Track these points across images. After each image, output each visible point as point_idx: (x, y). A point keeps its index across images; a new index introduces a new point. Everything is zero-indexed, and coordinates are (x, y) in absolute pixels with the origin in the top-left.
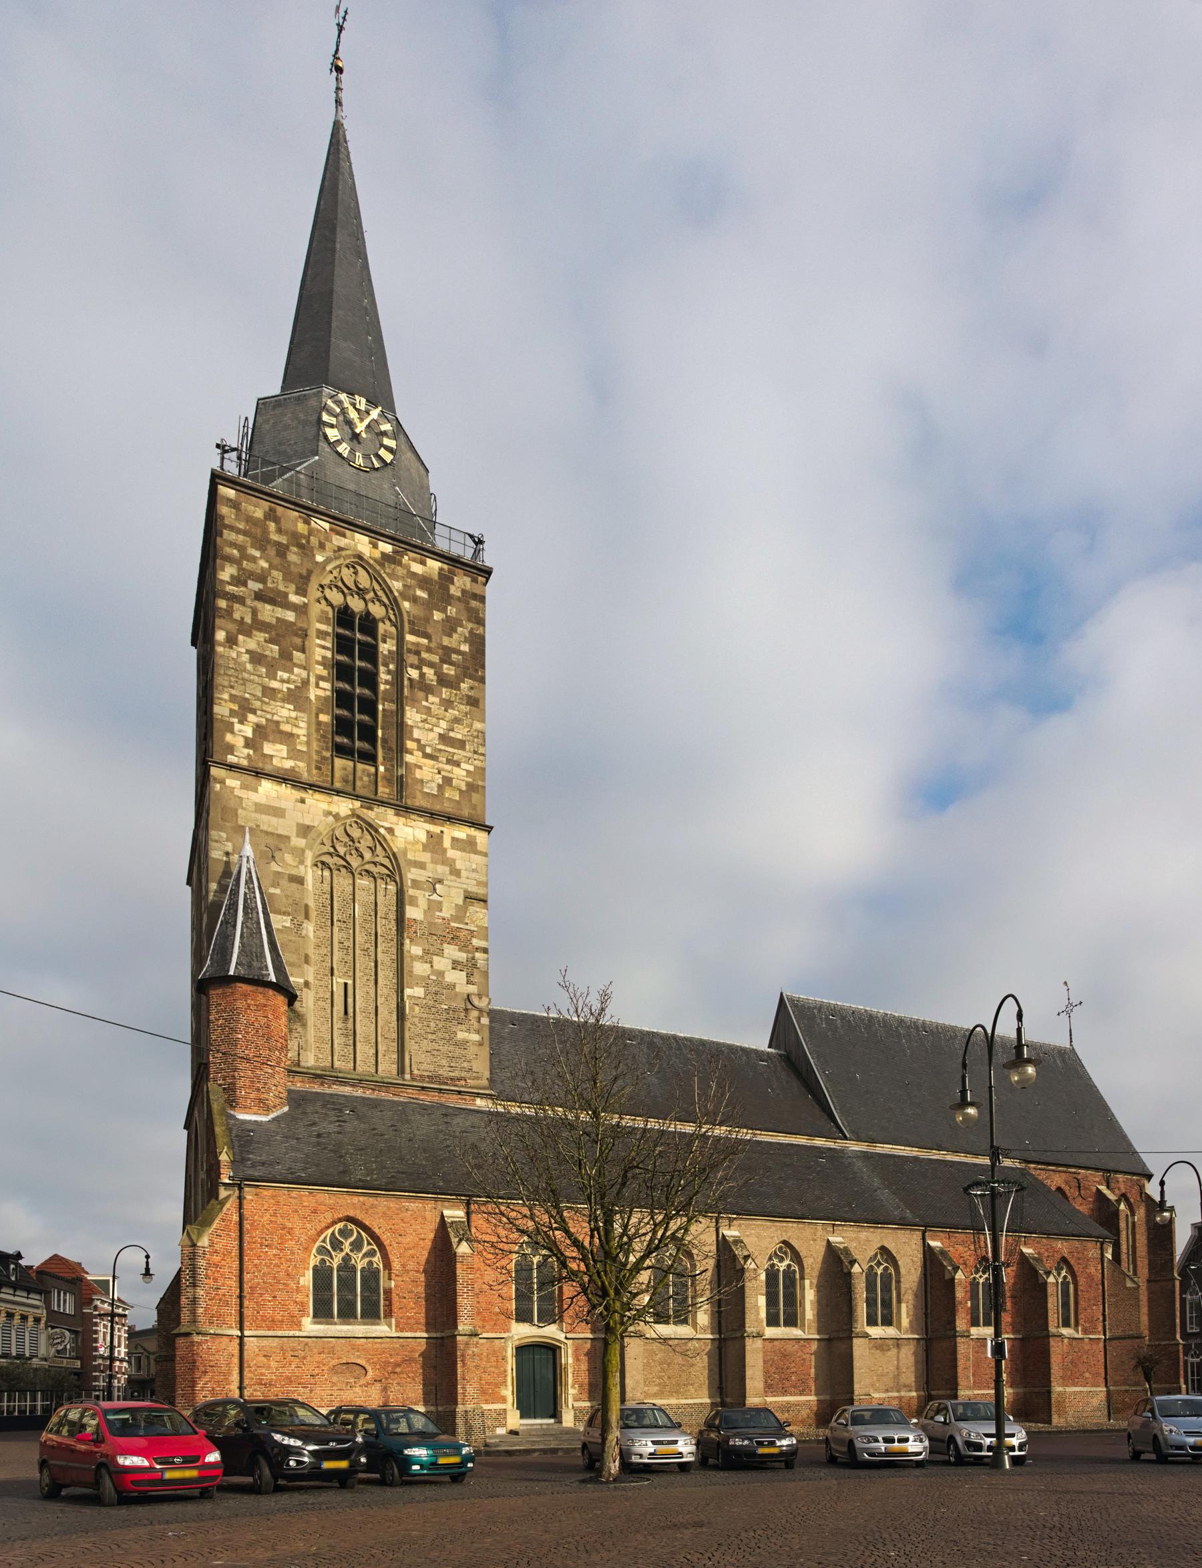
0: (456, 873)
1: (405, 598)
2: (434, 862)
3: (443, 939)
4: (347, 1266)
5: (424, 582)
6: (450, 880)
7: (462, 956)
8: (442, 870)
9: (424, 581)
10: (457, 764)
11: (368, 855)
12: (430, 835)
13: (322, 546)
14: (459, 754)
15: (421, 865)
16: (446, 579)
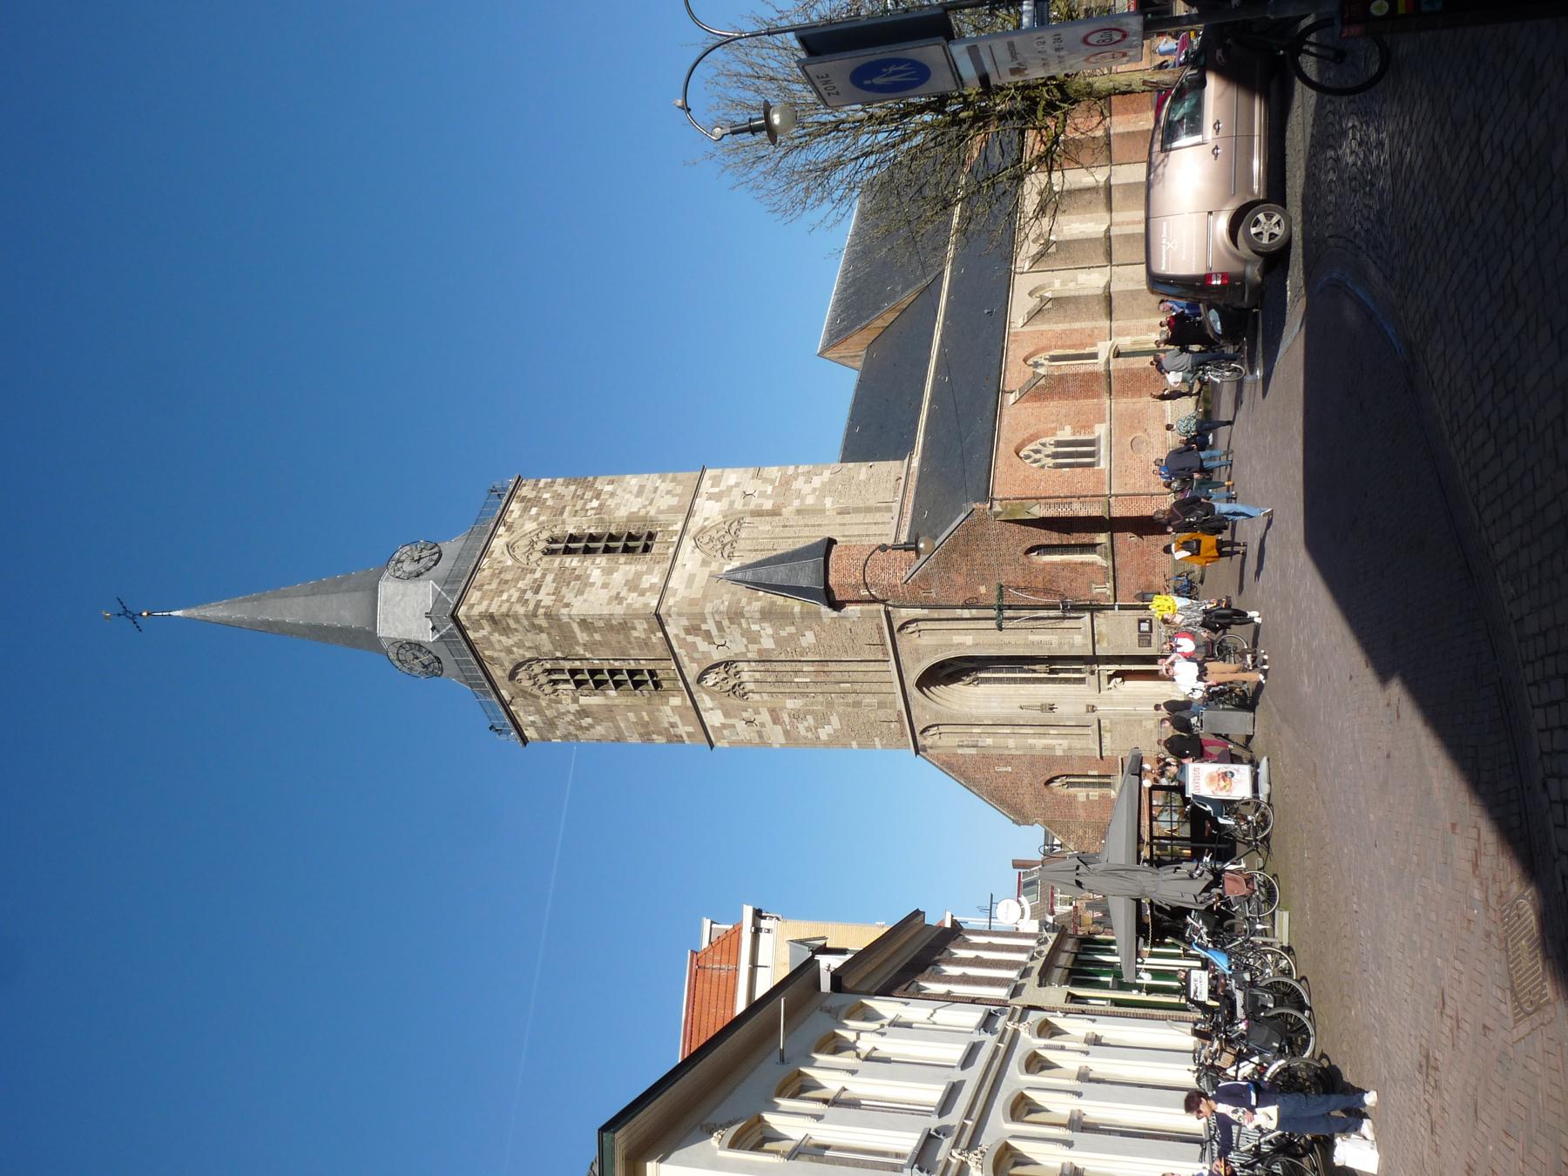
5: (525, 510)
7: (801, 479)
15: (732, 503)
16: (523, 499)
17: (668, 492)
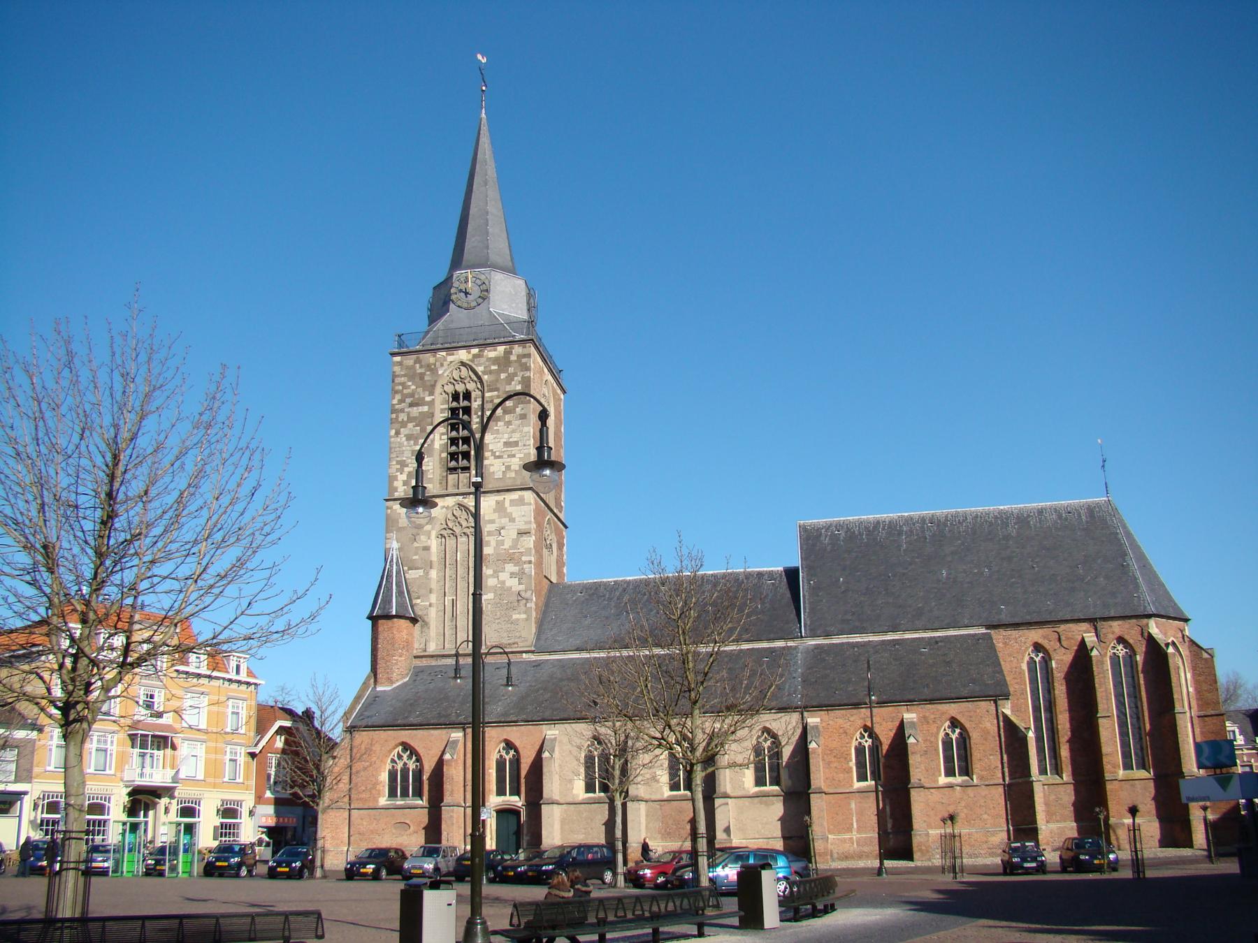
0: (512, 520)
1: (484, 373)
2: (500, 517)
3: (505, 562)
4: (405, 770)
6: (509, 526)
7: (516, 569)
8: (505, 521)
9: (496, 361)
10: (514, 456)
11: (464, 524)
12: (498, 503)
13: (442, 365)
14: (514, 450)
15: (492, 522)
16: (508, 353)
17: (508, 468)
